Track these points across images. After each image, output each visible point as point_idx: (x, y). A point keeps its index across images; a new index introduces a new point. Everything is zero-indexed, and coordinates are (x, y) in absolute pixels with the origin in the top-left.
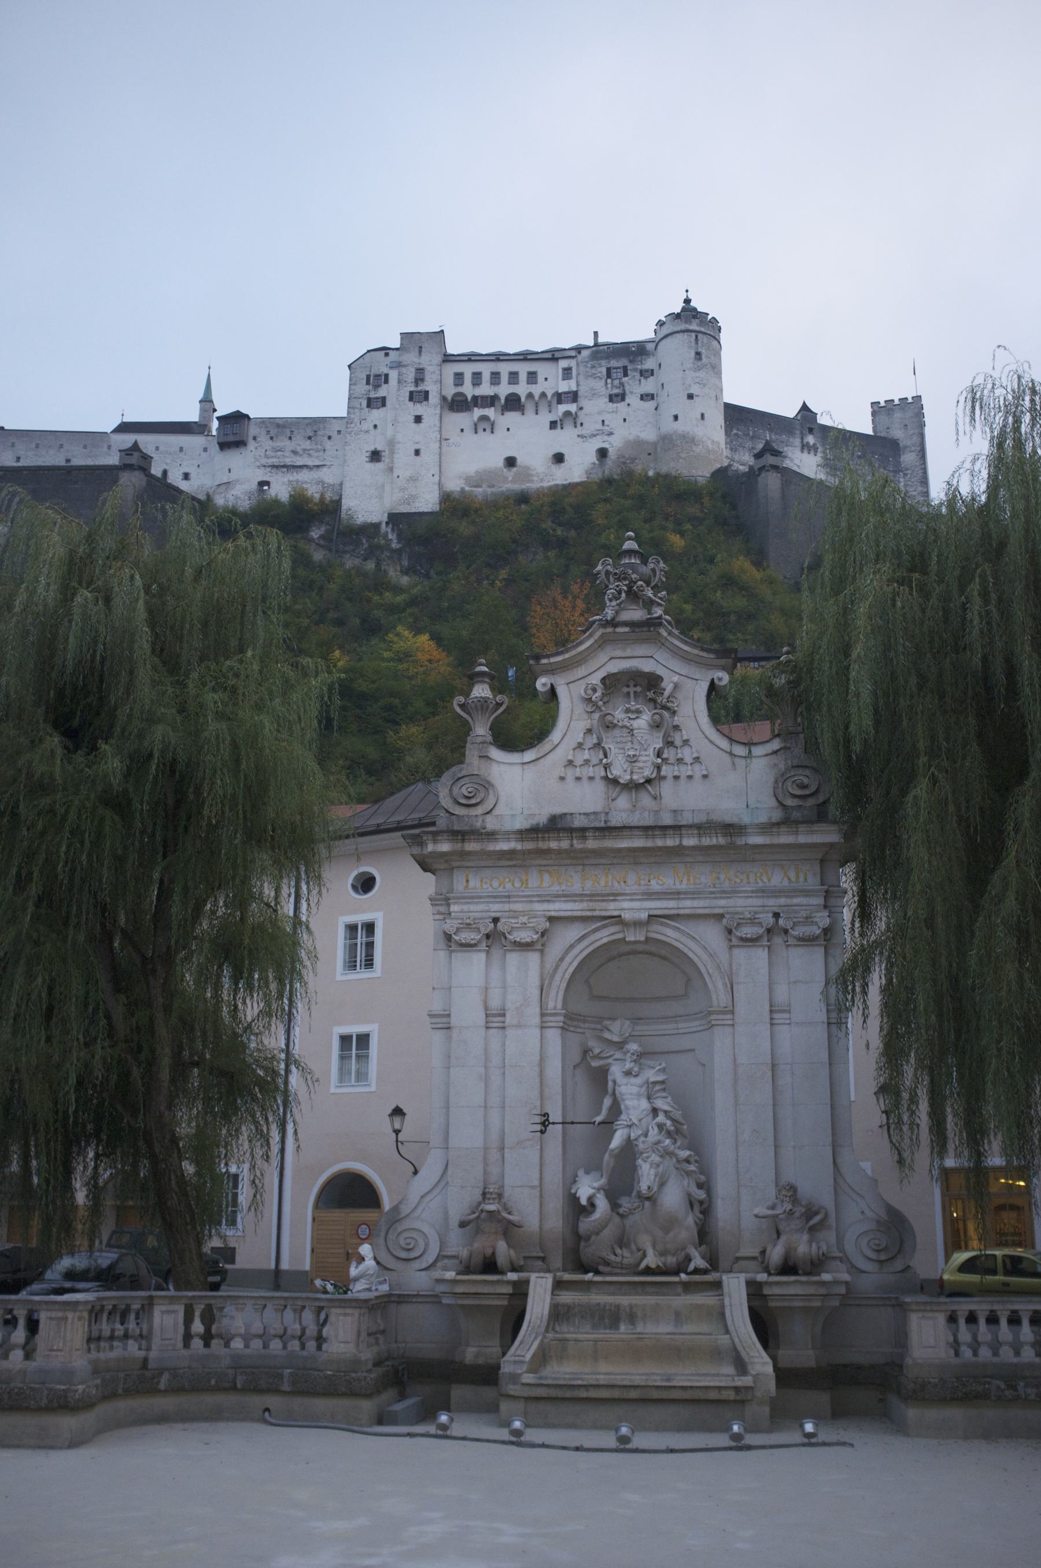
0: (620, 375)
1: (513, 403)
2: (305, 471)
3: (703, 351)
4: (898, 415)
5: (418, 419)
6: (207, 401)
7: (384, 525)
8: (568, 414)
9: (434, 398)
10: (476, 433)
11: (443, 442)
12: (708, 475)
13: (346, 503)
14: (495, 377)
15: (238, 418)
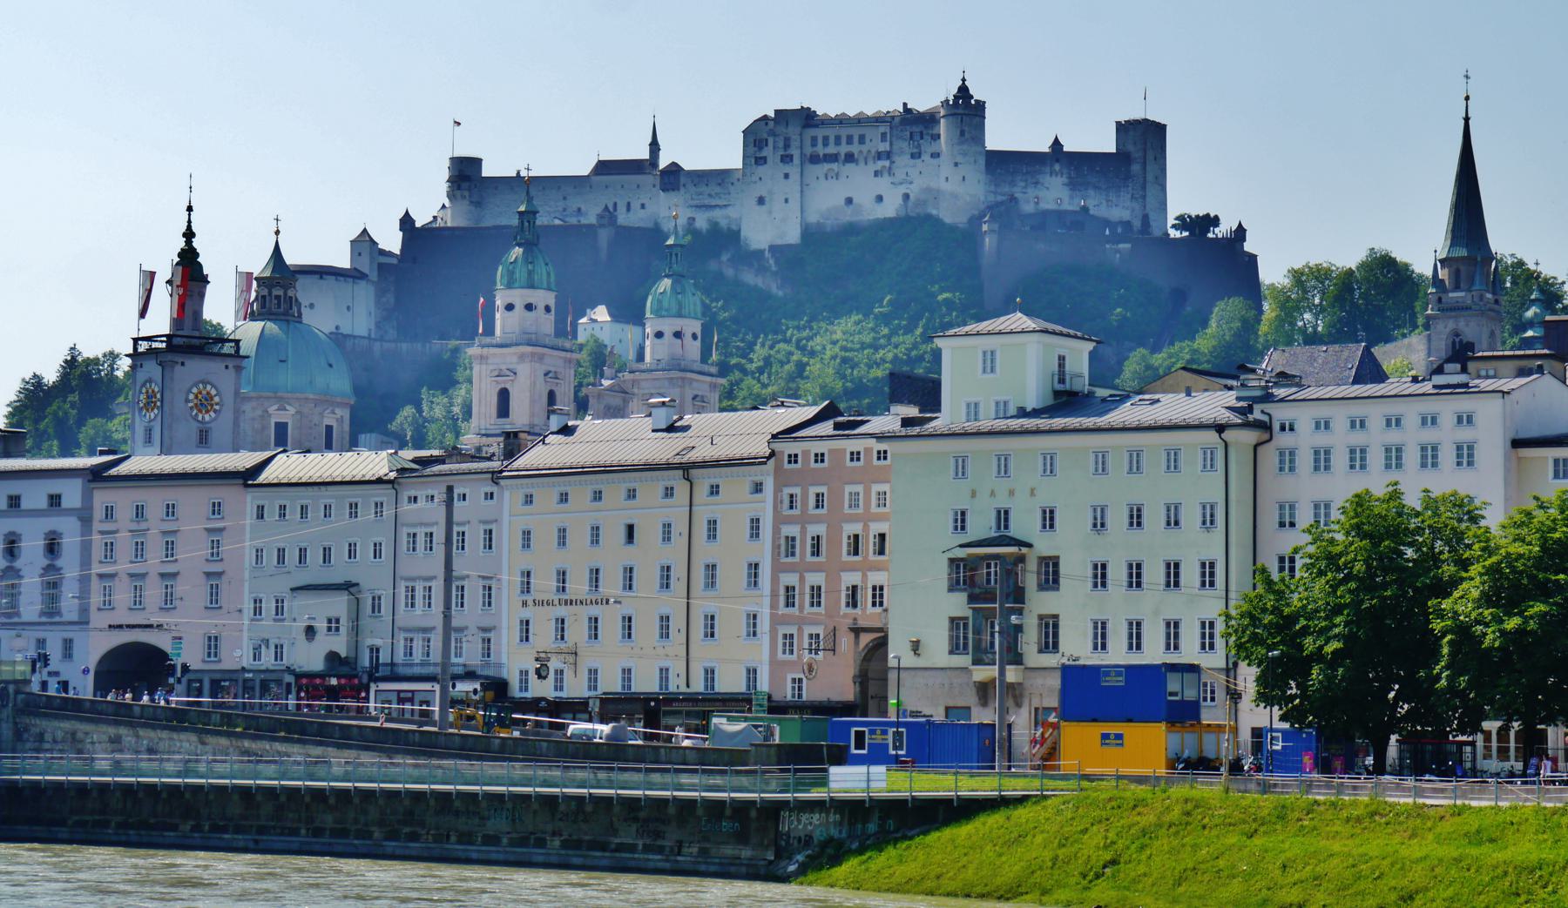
0: (919, 138)
1: (850, 158)
2: (718, 209)
3: (966, 129)
4: (1131, 133)
5: (786, 176)
6: (654, 146)
7: (767, 252)
8: (884, 167)
9: (796, 160)
10: (827, 179)
11: (805, 187)
12: (965, 220)
13: (742, 234)
14: (838, 140)
15: (674, 169)
